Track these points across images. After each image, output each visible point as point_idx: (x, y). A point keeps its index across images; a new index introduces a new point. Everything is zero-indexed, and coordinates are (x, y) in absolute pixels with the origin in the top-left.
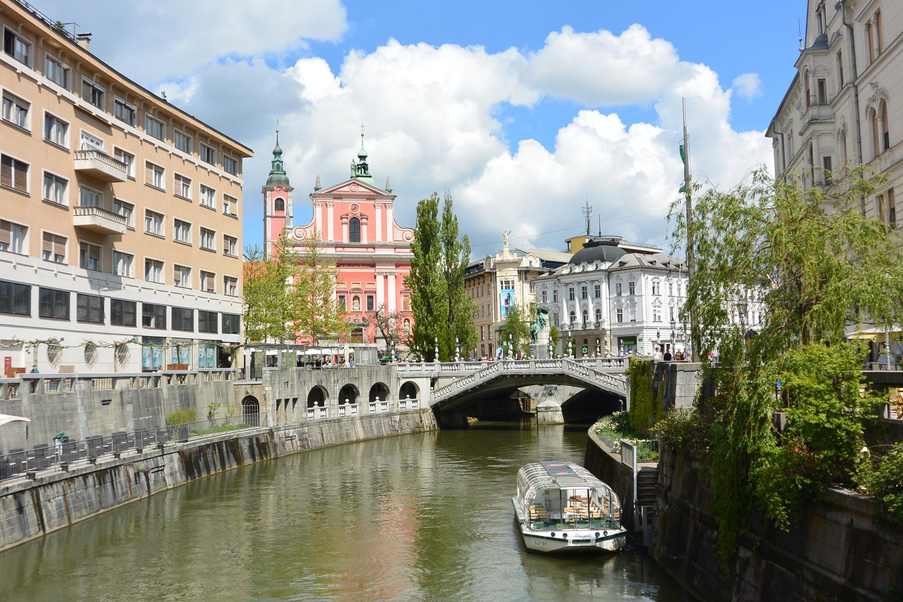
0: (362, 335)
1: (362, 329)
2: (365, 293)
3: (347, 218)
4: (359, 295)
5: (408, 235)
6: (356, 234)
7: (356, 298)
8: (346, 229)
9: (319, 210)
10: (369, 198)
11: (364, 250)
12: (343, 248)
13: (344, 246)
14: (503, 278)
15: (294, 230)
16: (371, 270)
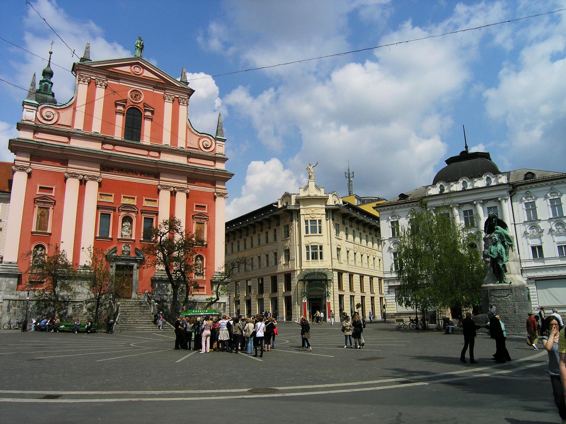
0: (132, 276)
1: (132, 266)
2: (142, 213)
3: (124, 106)
4: (133, 215)
5: (207, 143)
6: (135, 130)
7: (127, 219)
8: (120, 120)
9: (83, 89)
10: (157, 85)
11: (145, 153)
12: (114, 145)
13: (115, 143)
14: (309, 216)
15: (40, 108)
16: (154, 182)
